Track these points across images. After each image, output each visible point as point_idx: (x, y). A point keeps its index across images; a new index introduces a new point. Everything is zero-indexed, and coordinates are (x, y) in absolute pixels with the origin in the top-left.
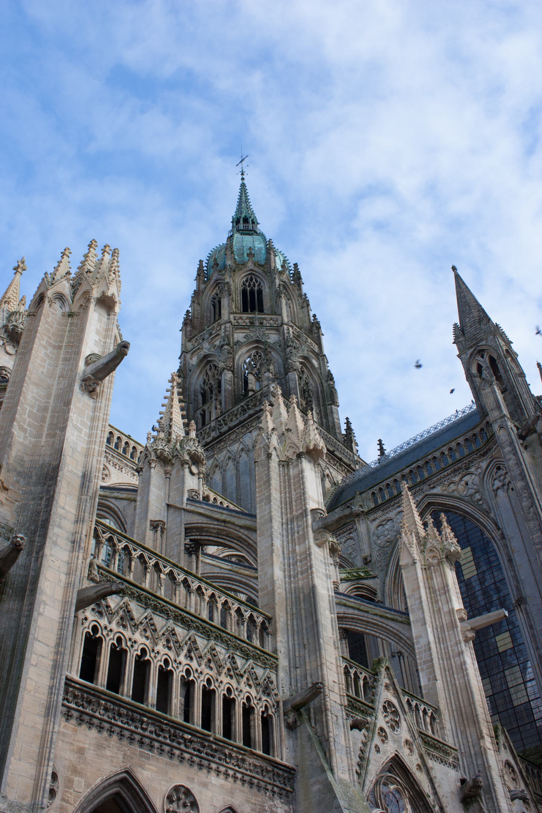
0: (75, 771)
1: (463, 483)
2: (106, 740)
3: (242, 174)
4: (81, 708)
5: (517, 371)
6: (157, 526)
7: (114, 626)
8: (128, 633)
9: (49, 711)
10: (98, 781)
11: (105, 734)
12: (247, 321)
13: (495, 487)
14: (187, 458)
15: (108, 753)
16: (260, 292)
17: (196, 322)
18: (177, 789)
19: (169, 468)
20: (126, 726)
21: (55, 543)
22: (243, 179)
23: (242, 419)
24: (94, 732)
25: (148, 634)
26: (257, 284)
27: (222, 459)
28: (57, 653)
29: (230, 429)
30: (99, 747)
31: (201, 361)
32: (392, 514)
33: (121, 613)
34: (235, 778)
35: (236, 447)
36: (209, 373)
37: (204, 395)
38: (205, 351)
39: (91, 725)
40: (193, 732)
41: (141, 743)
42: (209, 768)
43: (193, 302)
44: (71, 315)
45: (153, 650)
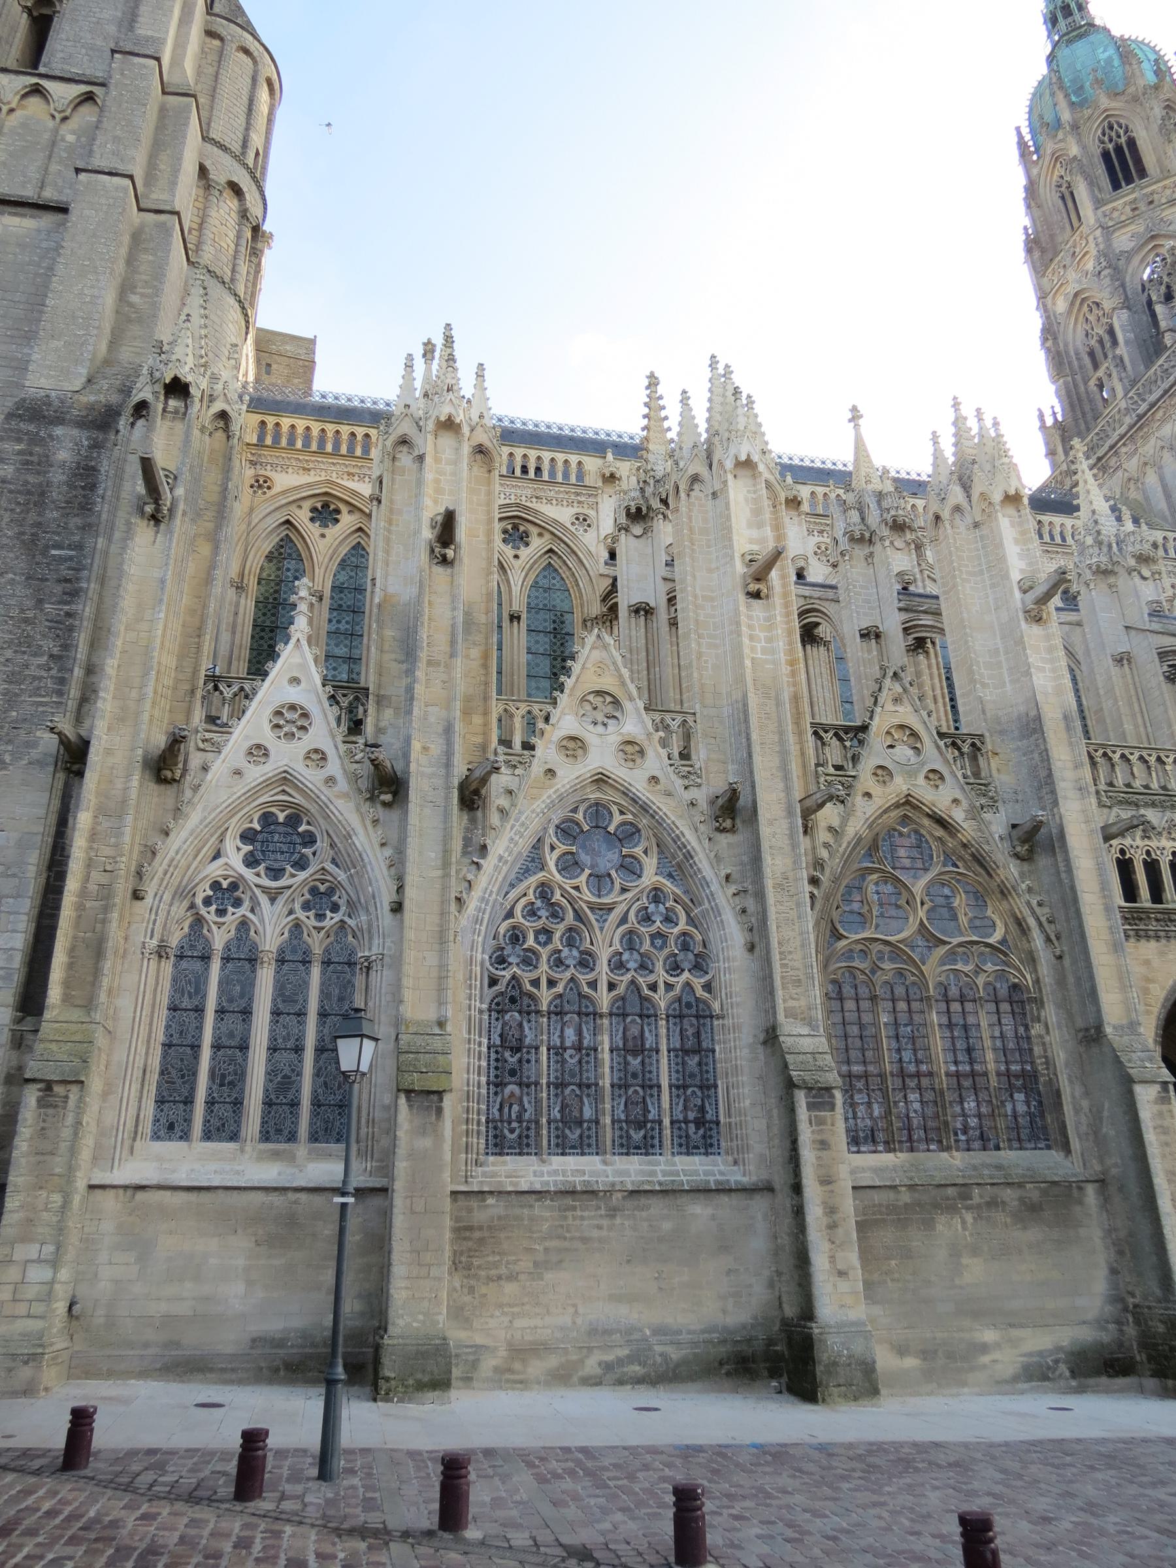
0: (1148, 980)
6: (1121, 660)
7: (1139, 842)
8: (1154, 844)
9: (1116, 948)
11: (1164, 941)
12: (1128, 209)
14: (1132, 562)
16: (1132, 143)
17: (1044, 239)
19: (1112, 580)
21: (1066, 798)
23: (1166, 385)
24: (1153, 944)
26: (1122, 132)
28: (1104, 897)
29: (1152, 406)
30: (1162, 954)
31: (1072, 304)
36: (1091, 318)
37: (1092, 354)
38: (1071, 289)
39: (1148, 937)
43: (1028, 207)
44: (976, 525)
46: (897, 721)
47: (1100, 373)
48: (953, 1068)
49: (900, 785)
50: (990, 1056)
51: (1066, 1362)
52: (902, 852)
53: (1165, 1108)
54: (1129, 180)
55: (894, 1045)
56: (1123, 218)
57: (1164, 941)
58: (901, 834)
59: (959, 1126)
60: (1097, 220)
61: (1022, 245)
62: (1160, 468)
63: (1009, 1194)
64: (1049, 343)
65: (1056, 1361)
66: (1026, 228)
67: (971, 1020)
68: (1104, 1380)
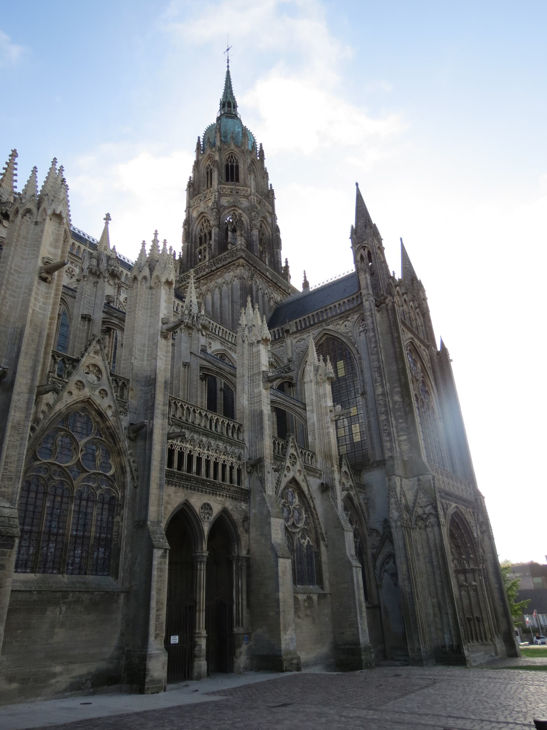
1: (344, 325)
3: (228, 62)
5: (382, 260)
6: (186, 365)
7: (179, 443)
8: (184, 445)
9: (160, 487)
10: (176, 505)
11: (177, 487)
12: (229, 190)
13: (360, 330)
14: (200, 327)
15: (179, 494)
16: (237, 167)
17: (196, 185)
18: (204, 504)
19: (190, 331)
21: (157, 417)
22: (228, 66)
23: (224, 263)
24: (173, 488)
27: (212, 286)
28: (161, 464)
29: (217, 269)
30: (175, 493)
31: (199, 216)
32: (305, 336)
34: (226, 496)
35: (220, 280)
36: (204, 225)
37: (201, 239)
38: (201, 209)
39: (172, 485)
40: (210, 482)
41: (191, 489)
42: (216, 494)
43: (194, 170)
44: (151, 288)
46: (93, 362)
47: (202, 248)
48: (75, 533)
49: (87, 392)
50: (93, 529)
52: (78, 424)
54: (232, 181)
55: (49, 518)
56: (227, 193)
58: (80, 416)
59: (70, 561)
60: (218, 189)
61: (187, 183)
62: (213, 294)
63: (86, 597)
64: (186, 227)
65: (86, 680)
66: (190, 177)
67: (89, 510)
68: (105, 687)
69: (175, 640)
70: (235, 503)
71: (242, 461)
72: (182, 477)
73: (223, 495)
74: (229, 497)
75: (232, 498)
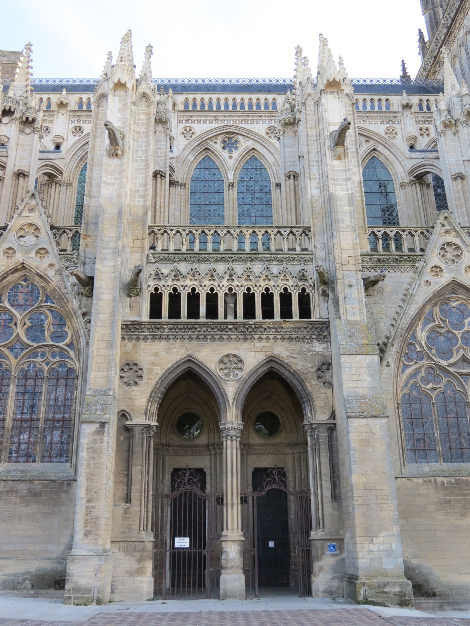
0: (153, 364)
2: (172, 344)
4: (153, 333)
10: (170, 365)
15: (174, 350)
20: (185, 333)
24: (164, 343)
25: (196, 278)
30: (168, 349)
33: (174, 273)
34: (275, 338)
39: (161, 339)
45: (201, 286)
46: (27, 221)
48: (19, 416)
49: (19, 257)
50: (42, 409)
51: (30, 580)
52: (21, 296)
53: (98, 437)
57: (171, 341)
58: (22, 286)
59: (14, 448)
63: (22, 487)
65: (24, 580)
67: (37, 389)
68: (52, 591)
69: (183, 542)
70: (298, 346)
71: (310, 282)
72: (186, 327)
73: (268, 338)
74: (283, 339)
75: (290, 339)
